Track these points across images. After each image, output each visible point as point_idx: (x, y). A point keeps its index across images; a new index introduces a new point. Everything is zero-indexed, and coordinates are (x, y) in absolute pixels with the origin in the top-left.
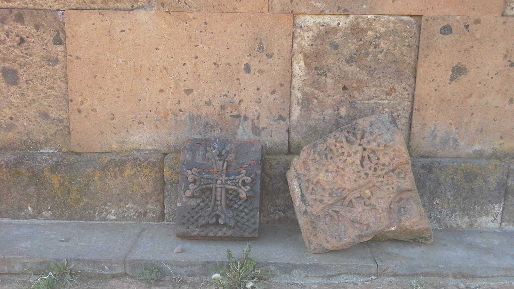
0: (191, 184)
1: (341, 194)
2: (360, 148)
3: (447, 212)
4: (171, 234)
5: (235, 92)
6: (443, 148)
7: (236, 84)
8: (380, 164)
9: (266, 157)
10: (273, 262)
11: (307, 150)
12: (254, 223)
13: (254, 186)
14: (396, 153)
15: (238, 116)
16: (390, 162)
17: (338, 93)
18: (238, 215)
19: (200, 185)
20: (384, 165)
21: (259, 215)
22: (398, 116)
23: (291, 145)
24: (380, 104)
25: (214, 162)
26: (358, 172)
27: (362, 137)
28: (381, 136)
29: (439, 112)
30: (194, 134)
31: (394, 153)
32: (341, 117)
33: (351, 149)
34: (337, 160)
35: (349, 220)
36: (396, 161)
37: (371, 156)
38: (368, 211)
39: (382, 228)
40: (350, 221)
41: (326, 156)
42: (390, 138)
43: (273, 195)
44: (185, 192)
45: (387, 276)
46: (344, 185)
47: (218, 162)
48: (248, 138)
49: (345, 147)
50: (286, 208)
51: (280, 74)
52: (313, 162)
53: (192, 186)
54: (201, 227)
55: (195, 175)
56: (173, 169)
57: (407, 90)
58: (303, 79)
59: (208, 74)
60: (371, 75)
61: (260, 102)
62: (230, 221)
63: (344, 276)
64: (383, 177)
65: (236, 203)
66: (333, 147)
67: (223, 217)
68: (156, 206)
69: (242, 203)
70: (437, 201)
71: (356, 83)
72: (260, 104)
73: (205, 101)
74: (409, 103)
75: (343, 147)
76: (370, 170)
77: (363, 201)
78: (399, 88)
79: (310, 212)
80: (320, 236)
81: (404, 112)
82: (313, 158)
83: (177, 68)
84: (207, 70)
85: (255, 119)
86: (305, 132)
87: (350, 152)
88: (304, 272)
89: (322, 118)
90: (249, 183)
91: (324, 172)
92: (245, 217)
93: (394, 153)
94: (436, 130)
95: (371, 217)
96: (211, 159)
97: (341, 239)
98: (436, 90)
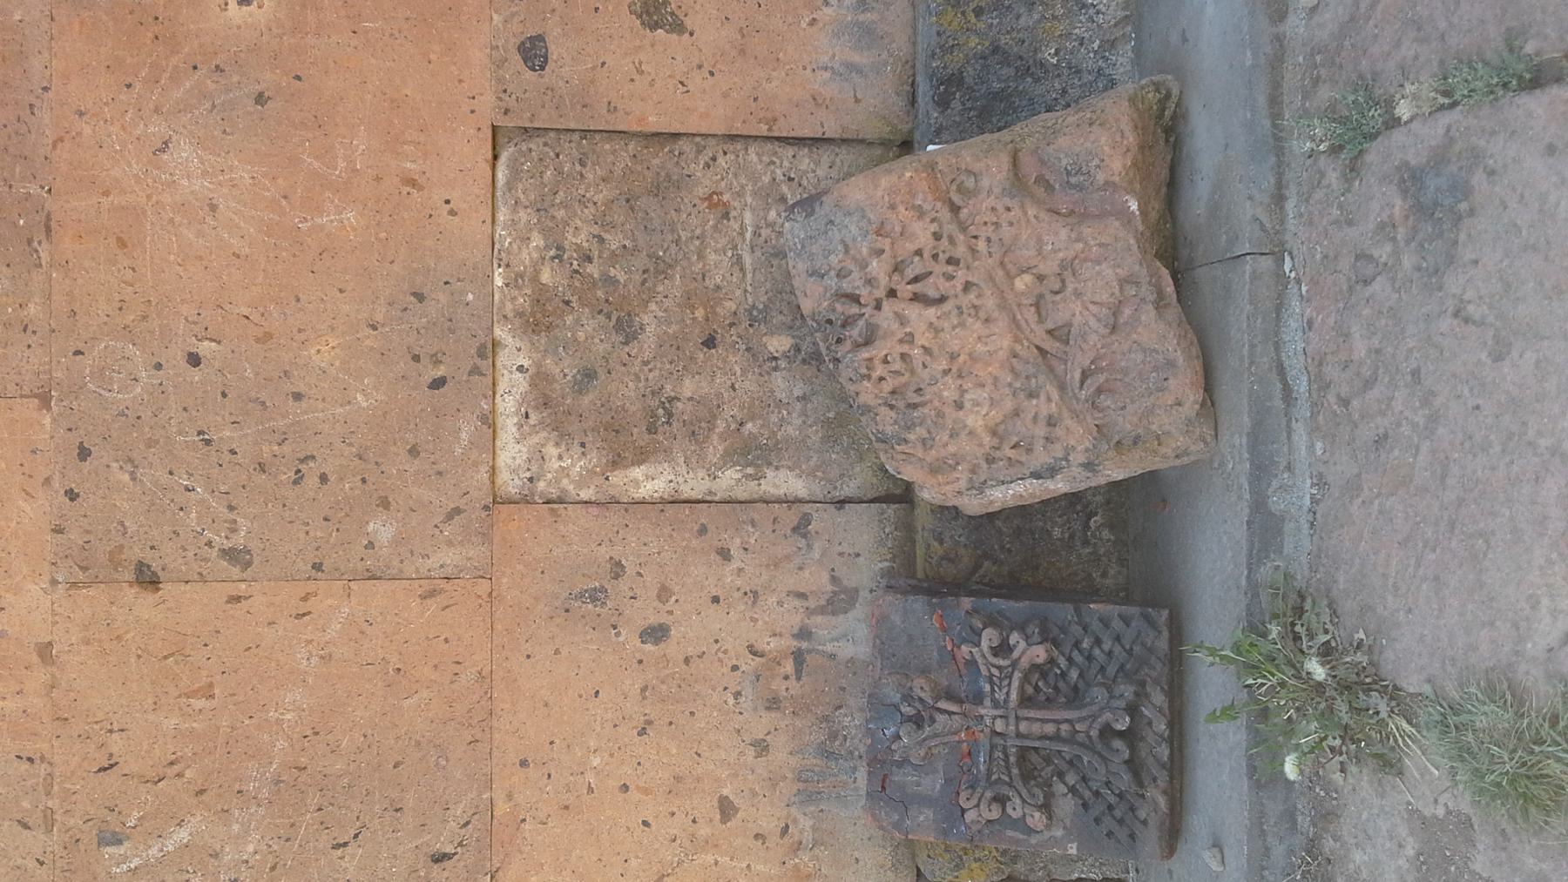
0: (1009, 810)
1: (1028, 363)
2: (886, 305)
3: (1081, 22)
4: (1166, 867)
5: (726, 670)
6: (886, 41)
7: (702, 666)
8: (934, 248)
9: (920, 574)
10: (1246, 573)
11: (896, 461)
12: (1126, 621)
14: (902, 202)
15: (799, 657)
16: (928, 220)
17: (725, 361)
18: (1102, 669)
19: (1010, 785)
20: (937, 236)
22: (791, 179)
23: (883, 493)
24: (756, 234)
25: (938, 739)
26: (962, 313)
27: (855, 299)
28: (851, 245)
29: (778, 59)
30: (856, 789)
31: (901, 209)
32: (798, 349)
33: (893, 333)
34: (925, 374)
35: (1109, 340)
36: (924, 201)
37: (910, 273)
38: (1079, 282)
39: (1132, 241)
40: (1113, 338)
41: (914, 406)
42: (855, 219)
43: (1038, 550)
44: (1030, 831)
45: (1282, 222)
46: (1002, 355)
47: (938, 727)
48: (864, 625)
49: (884, 353)
50: (1079, 507)
51: (671, 536)
52: (932, 446)
53: (1014, 809)
54: (1141, 784)
55: (980, 800)
56: (964, 857)
57: (714, 159)
58: (683, 465)
59: (674, 751)
60: (670, 266)
61: (755, 593)
63: (1283, 354)
64: (975, 237)
65: (1064, 674)
66: (887, 387)
67: (1108, 716)
69: (1064, 655)
70: (1048, 55)
71: (693, 308)
72: (760, 593)
73: (756, 757)
74: (751, 150)
75: (886, 356)
76: (954, 277)
77: (1049, 297)
78: (708, 183)
79: (1087, 455)
80: (1161, 426)
81: (778, 162)
82: (919, 445)
83: (656, 846)
84: (661, 754)
85: (806, 604)
86: (842, 454)
87: (899, 335)
88: (1277, 475)
89: (798, 406)
90: (1001, 634)
91: (961, 413)
93: (901, 209)
94: (830, 65)
95: (1098, 273)
96: (930, 748)
97: (1171, 364)
98: (712, 74)
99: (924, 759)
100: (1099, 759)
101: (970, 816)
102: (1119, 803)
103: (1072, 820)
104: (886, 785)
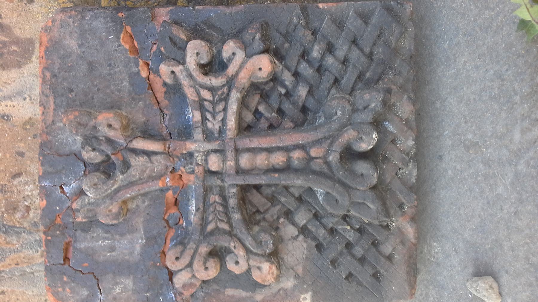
0: (231, 266)
13: (220, 31)
18: (336, 81)
19: (231, 234)
21: (330, 5)
25: (136, 188)
44: (256, 286)
47: (134, 173)
53: (237, 263)
55: (193, 258)
62: (365, 108)
65: (288, 95)
67: (350, 134)
69: (289, 69)
92: (341, 53)
99: (117, 216)
100: (341, 189)
101: (180, 280)
102: (359, 240)
103: (304, 268)
104: (70, 255)
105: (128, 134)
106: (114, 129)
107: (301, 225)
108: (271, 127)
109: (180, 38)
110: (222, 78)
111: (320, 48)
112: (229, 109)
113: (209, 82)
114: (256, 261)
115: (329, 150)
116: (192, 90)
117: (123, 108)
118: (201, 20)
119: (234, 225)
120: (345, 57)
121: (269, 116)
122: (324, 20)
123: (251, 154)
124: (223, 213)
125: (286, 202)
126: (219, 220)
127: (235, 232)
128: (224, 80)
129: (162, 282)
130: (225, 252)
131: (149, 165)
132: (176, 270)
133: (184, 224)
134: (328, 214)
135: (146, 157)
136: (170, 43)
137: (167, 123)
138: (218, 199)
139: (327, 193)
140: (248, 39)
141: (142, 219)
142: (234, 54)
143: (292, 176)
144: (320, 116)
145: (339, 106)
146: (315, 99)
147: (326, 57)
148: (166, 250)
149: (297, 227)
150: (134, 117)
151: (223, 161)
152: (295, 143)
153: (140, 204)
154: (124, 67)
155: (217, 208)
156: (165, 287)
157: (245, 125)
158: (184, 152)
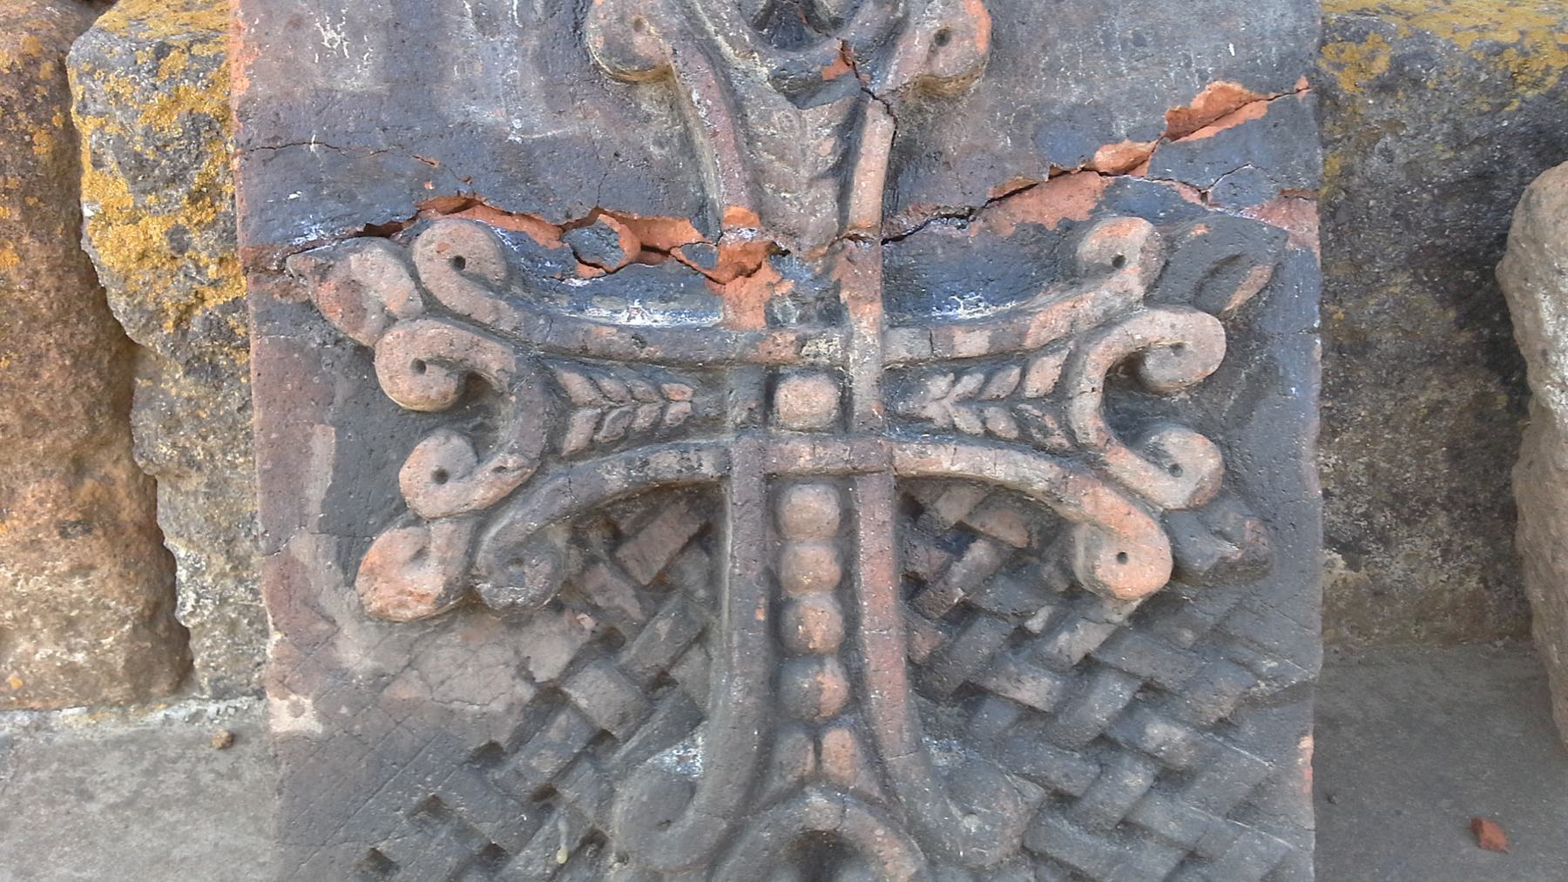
0: (430, 453)
13: (1241, 417)
18: (1062, 800)
21: (1308, 773)
25: (722, 121)
50: (1383, 518)
53: (441, 477)
55: (463, 320)
56: (179, 192)
68: (82, 569)
69: (1107, 644)
99: (618, 49)
100: (709, 839)
103: (413, 706)
105: (911, 101)
106: (933, 52)
107: (571, 691)
108: (913, 586)
109: (1234, 291)
110: (1099, 430)
111: (1176, 747)
112: (992, 454)
113: (1085, 385)
114: (450, 544)
115: (845, 791)
116: (1062, 327)
117: (993, 82)
118: (1277, 355)
119: (580, 464)
120: (1143, 828)
121: (955, 580)
122: (1262, 755)
123: (835, 527)
124: (627, 429)
125: (654, 637)
126: (603, 415)
127: (554, 468)
128: (1093, 438)
129: (362, 199)
130: (475, 429)
131: (804, 173)
132: (416, 258)
133: (578, 283)
134: (609, 783)
135: (831, 161)
136: (1222, 257)
137: (936, 228)
138: (676, 411)
139: (692, 789)
140: (1224, 516)
141: (598, 134)
142: (1175, 469)
143: (759, 669)
144: (950, 750)
145: (993, 826)
146: (1006, 730)
147: (1145, 764)
148: (479, 216)
149: (561, 675)
150: (959, 119)
151: (810, 430)
152: (872, 678)
153: (654, 127)
154: (1132, 88)
155: (646, 408)
156: (342, 209)
157: (924, 497)
158: (844, 295)
